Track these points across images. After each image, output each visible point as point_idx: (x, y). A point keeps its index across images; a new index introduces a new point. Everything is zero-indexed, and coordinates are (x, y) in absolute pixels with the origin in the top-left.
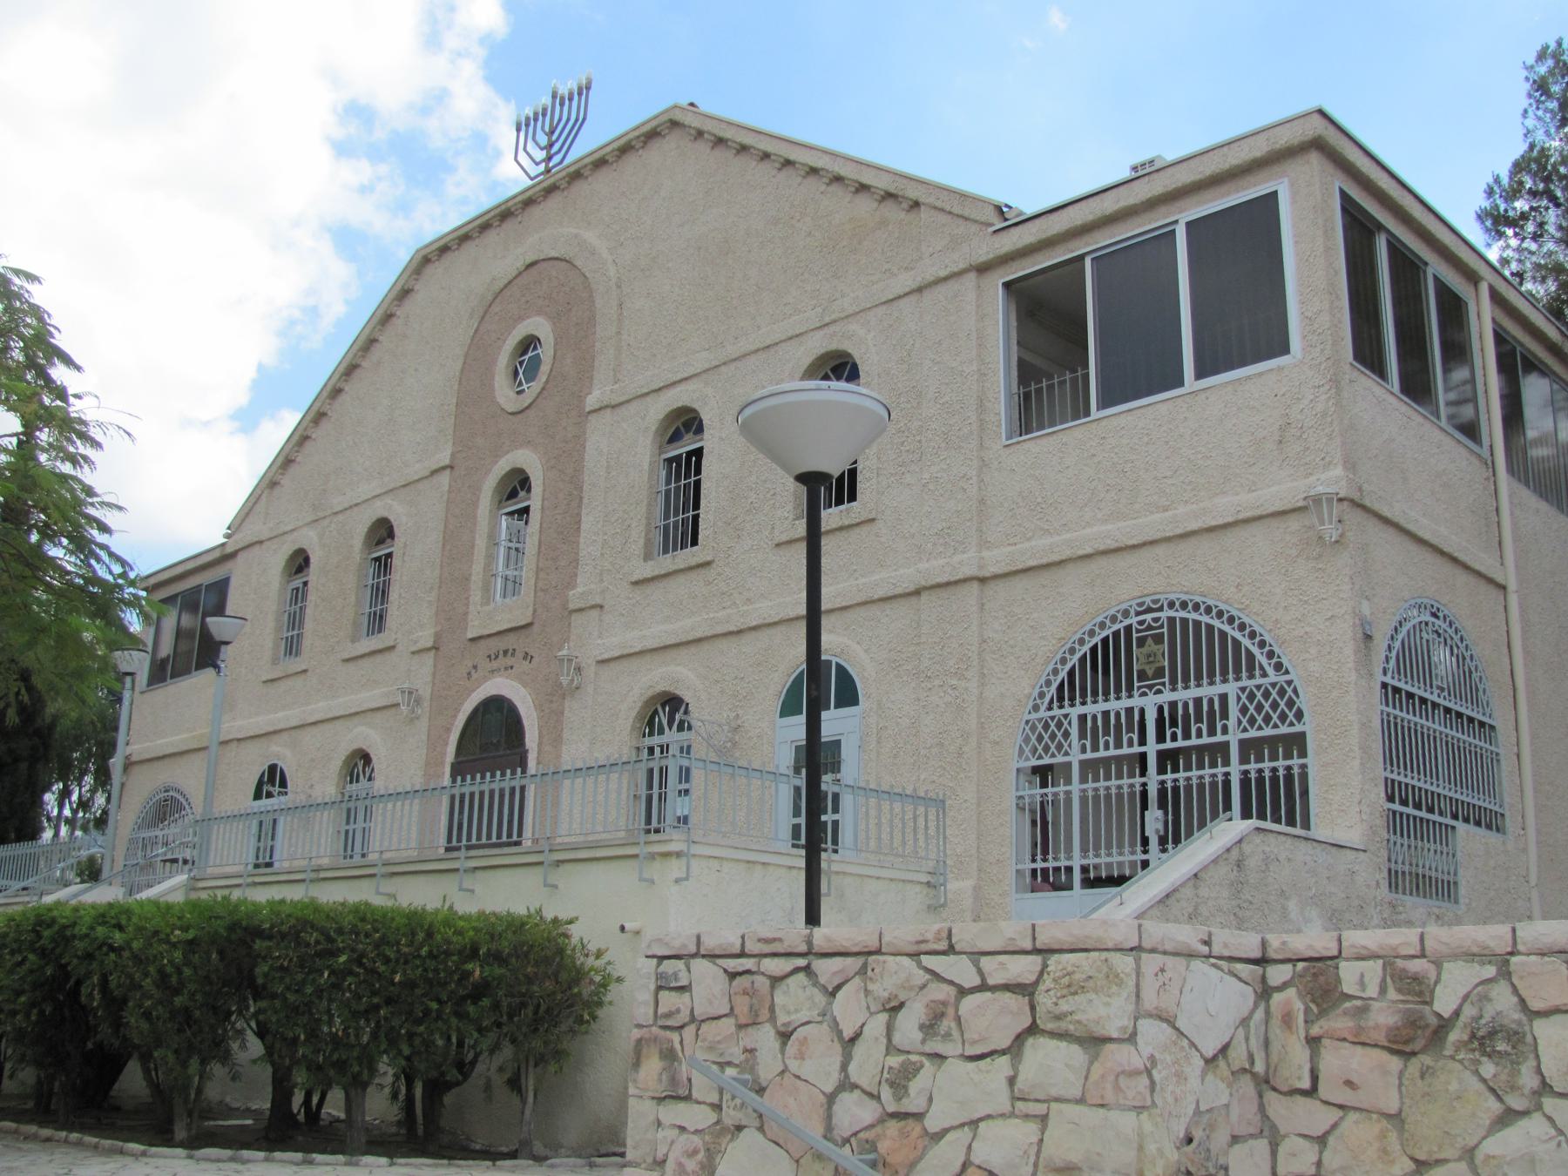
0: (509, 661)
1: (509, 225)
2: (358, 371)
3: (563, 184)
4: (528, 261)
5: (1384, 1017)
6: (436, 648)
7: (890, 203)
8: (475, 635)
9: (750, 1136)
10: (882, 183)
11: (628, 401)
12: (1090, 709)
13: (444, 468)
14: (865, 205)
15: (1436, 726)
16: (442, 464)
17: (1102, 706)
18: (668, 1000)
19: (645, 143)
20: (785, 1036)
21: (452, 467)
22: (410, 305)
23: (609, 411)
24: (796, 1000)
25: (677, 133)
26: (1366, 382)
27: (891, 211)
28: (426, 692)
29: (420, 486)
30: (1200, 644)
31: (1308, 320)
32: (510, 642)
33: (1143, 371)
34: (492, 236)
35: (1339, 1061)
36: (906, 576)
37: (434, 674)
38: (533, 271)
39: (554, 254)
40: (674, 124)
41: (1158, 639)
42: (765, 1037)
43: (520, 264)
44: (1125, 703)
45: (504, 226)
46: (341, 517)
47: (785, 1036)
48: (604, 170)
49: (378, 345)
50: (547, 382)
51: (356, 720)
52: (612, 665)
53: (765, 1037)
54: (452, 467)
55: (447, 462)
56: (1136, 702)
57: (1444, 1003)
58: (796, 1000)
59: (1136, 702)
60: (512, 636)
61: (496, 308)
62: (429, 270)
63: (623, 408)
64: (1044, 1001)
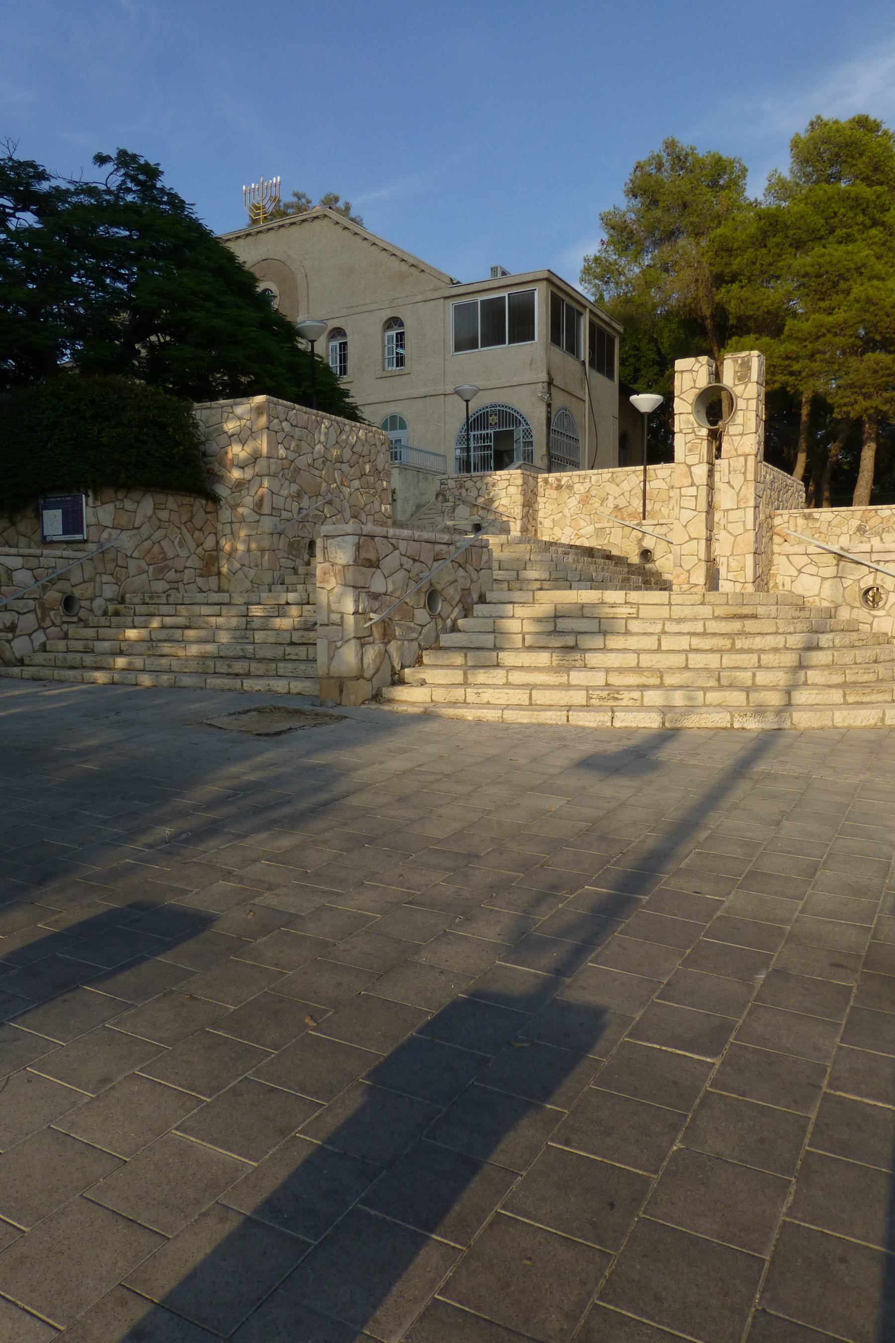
1: (249, 239)
5: (554, 485)
7: (413, 268)
9: (462, 506)
10: (411, 261)
12: (476, 433)
14: (404, 267)
15: (564, 439)
17: (479, 432)
18: (443, 486)
20: (467, 490)
24: (469, 484)
25: (326, 219)
26: (555, 349)
27: (412, 270)
30: (509, 417)
31: (539, 330)
33: (494, 337)
34: (241, 242)
35: (547, 492)
36: (422, 391)
40: (326, 216)
41: (495, 415)
42: (463, 491)
43: (259, 258)
44: (486, 432)
47: (467, 490)
48: (293, 228)
53: (463, 491)
56: (489, 431)
57: (563, 483)
58: (469, 484)
59: (489, 431)
64: (511, 481)
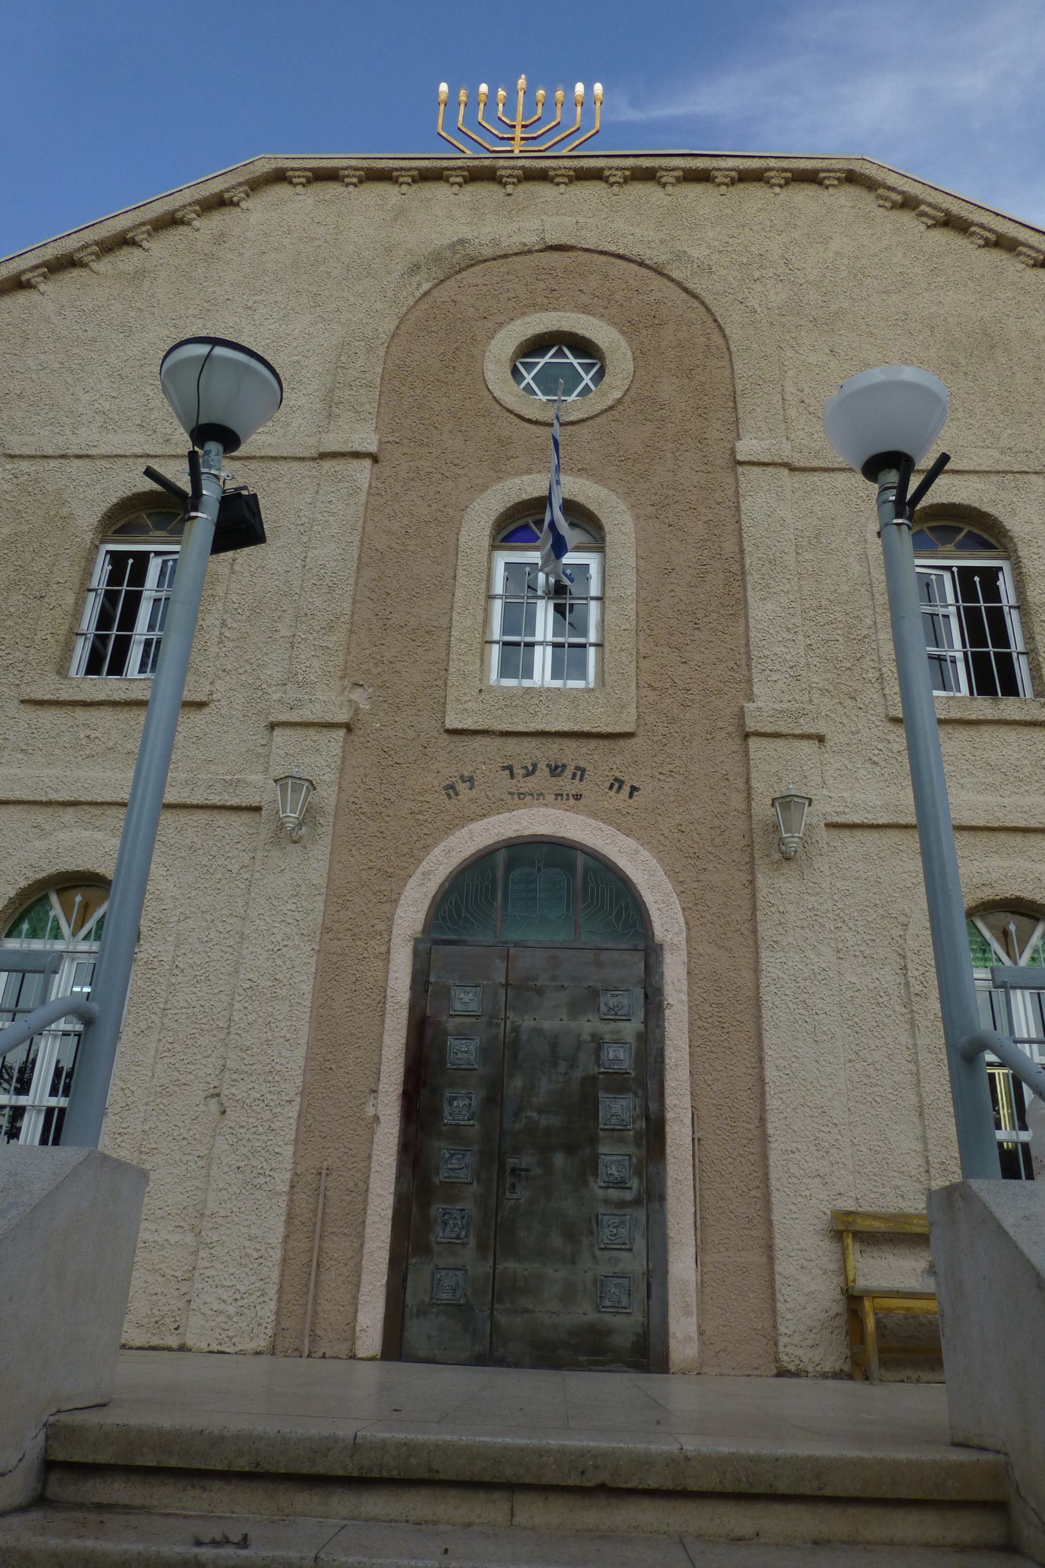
0: (566, 784)
2: (76, 272)
3: (618, 177)
4: (552, 239)
6: (348, 727)
8: (468, 724)
11: (833, 470)
13: (357, 455)
16: (357, 448)
19: (787, 182)
21: (375, 458)
22: (216, 221)
23: (786, 472)
28: (327, 795)
29: (283, 467)
32: (571, 753)
34: (440, 192)
37: (342, 771)
38: (556, 255)
39: (613, 248)
43: (531, 239)
45: (469, 188)
46: (24, 465)
49: (137, 252)
50: (619, 401)
51: (68, 815)
52: (859, 834)
54: (375, 458)
55: (373, 448)
60: (570, 744)
61: (469, 276)
62: (282, 191)
63: (816, 478)
